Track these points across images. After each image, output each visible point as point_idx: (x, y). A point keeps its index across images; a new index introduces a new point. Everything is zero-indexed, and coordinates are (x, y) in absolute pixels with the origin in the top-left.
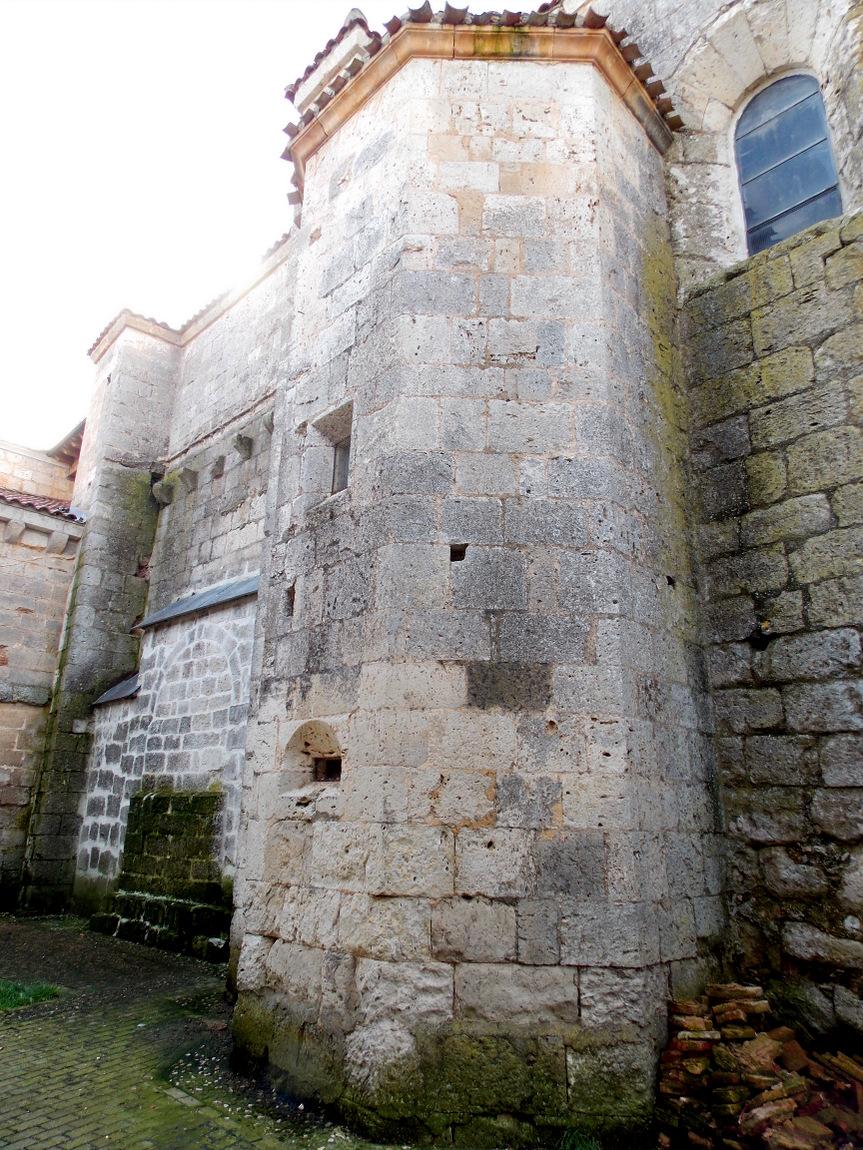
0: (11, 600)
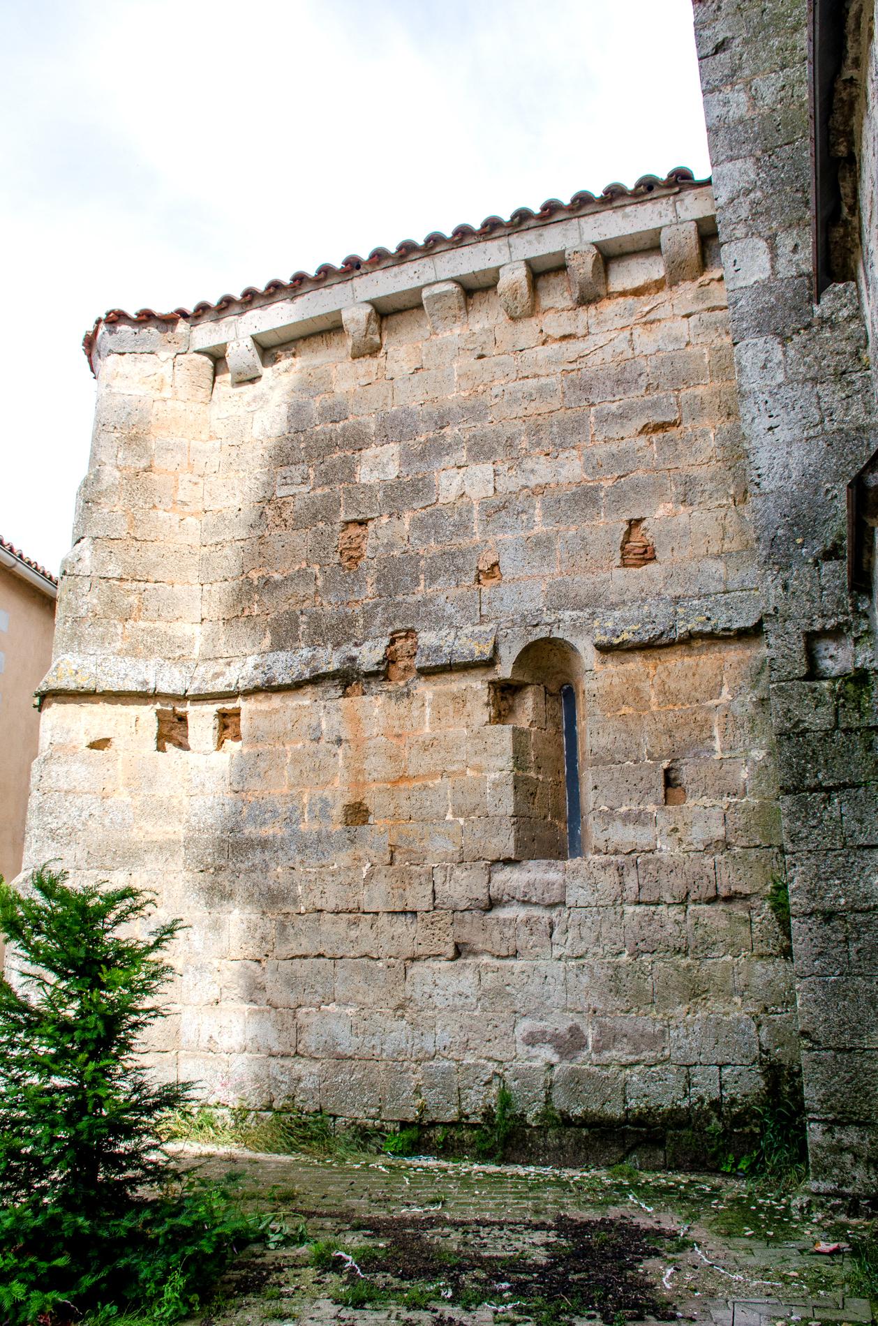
0: (623, 416)
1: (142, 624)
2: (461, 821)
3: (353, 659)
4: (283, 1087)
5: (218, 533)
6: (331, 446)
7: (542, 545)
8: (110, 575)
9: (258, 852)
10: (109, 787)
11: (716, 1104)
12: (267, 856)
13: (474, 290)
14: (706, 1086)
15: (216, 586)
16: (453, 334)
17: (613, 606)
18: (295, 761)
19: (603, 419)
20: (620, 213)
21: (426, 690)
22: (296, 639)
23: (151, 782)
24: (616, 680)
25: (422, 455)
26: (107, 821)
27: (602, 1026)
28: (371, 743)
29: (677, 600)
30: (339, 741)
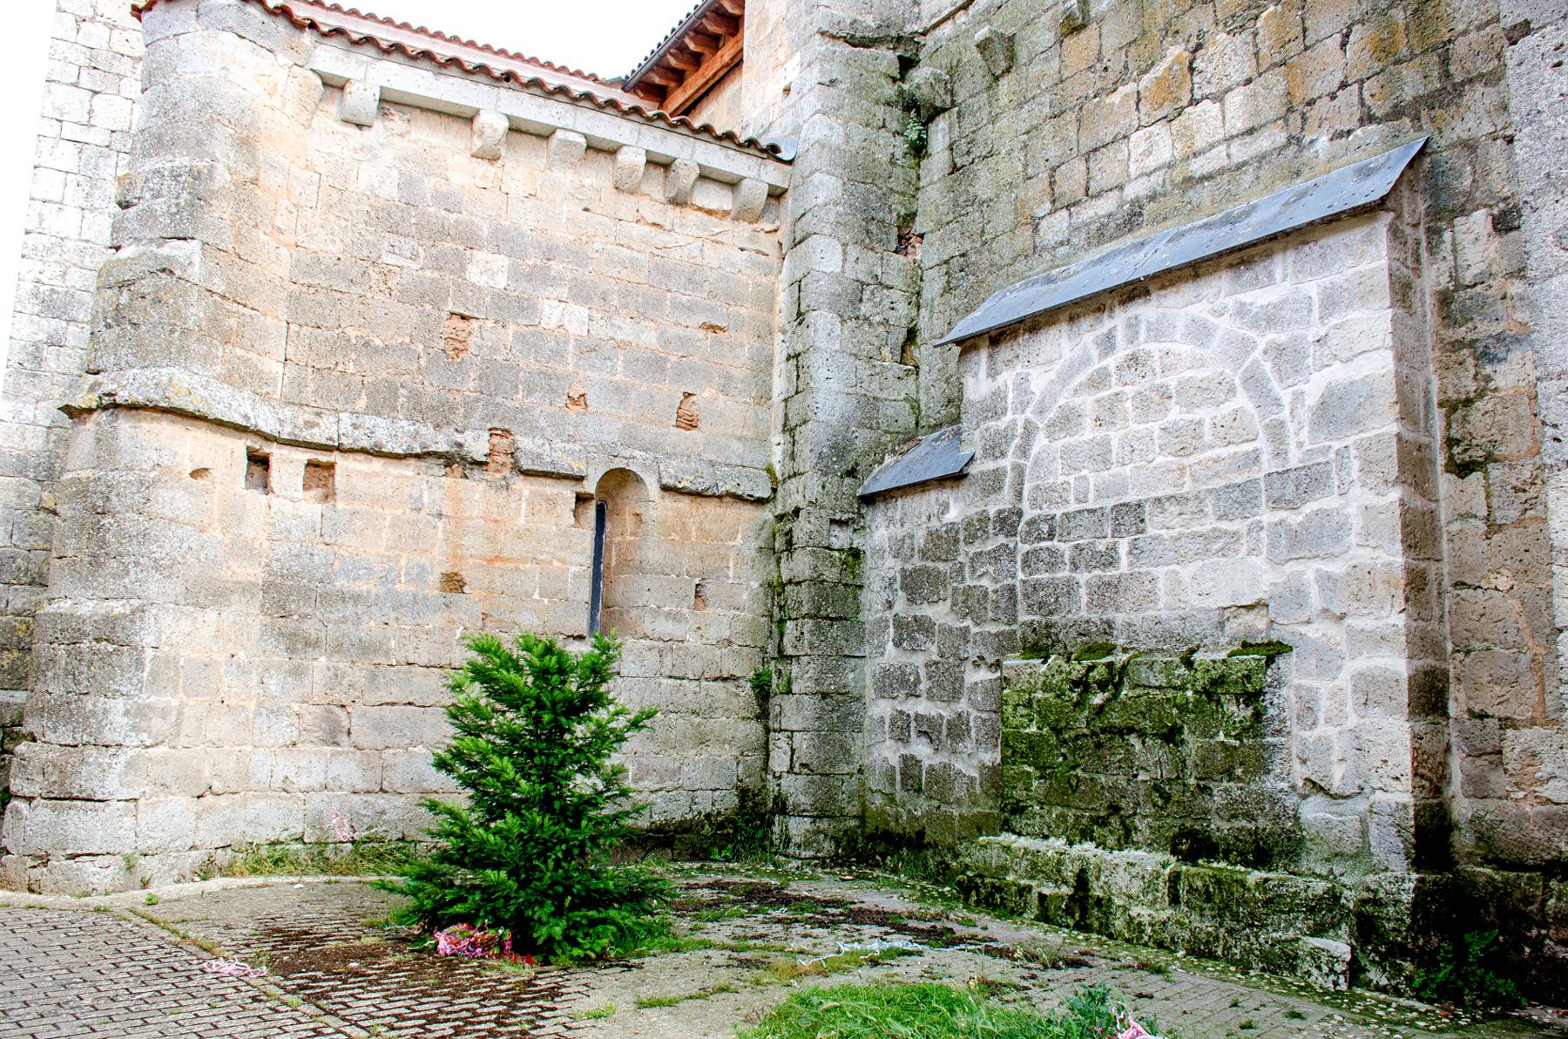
0: (690, 309)
1: (239, 352)
2: (546, 601)
3: (460, 445)
4: (366, 820)
5: (312, 276)
6: (443, 233)
7: (620, 391)
8: (214, 289)
9: (350, 606)
10: (206, 521)
11: (708, 816)
12: (360, 609)
13: (600, 150)
14: (705, 805)
15: (305, 330)
16: (566, 178)
17: (668, 456)
18: (393, 526)
19: (677, 306)
20: (724, 151)
21: (523, 486)
22: (394, 409)
23: (240, 521)
24: (670, 513)
25: (530, 277)
26: (202, 557)
27: (640, 764)
28: (470, 523)
29: (712, 464)
30: (440, 515)
